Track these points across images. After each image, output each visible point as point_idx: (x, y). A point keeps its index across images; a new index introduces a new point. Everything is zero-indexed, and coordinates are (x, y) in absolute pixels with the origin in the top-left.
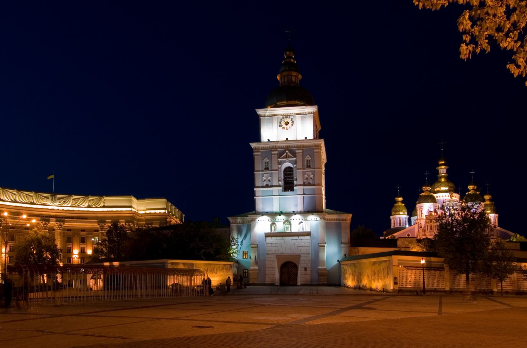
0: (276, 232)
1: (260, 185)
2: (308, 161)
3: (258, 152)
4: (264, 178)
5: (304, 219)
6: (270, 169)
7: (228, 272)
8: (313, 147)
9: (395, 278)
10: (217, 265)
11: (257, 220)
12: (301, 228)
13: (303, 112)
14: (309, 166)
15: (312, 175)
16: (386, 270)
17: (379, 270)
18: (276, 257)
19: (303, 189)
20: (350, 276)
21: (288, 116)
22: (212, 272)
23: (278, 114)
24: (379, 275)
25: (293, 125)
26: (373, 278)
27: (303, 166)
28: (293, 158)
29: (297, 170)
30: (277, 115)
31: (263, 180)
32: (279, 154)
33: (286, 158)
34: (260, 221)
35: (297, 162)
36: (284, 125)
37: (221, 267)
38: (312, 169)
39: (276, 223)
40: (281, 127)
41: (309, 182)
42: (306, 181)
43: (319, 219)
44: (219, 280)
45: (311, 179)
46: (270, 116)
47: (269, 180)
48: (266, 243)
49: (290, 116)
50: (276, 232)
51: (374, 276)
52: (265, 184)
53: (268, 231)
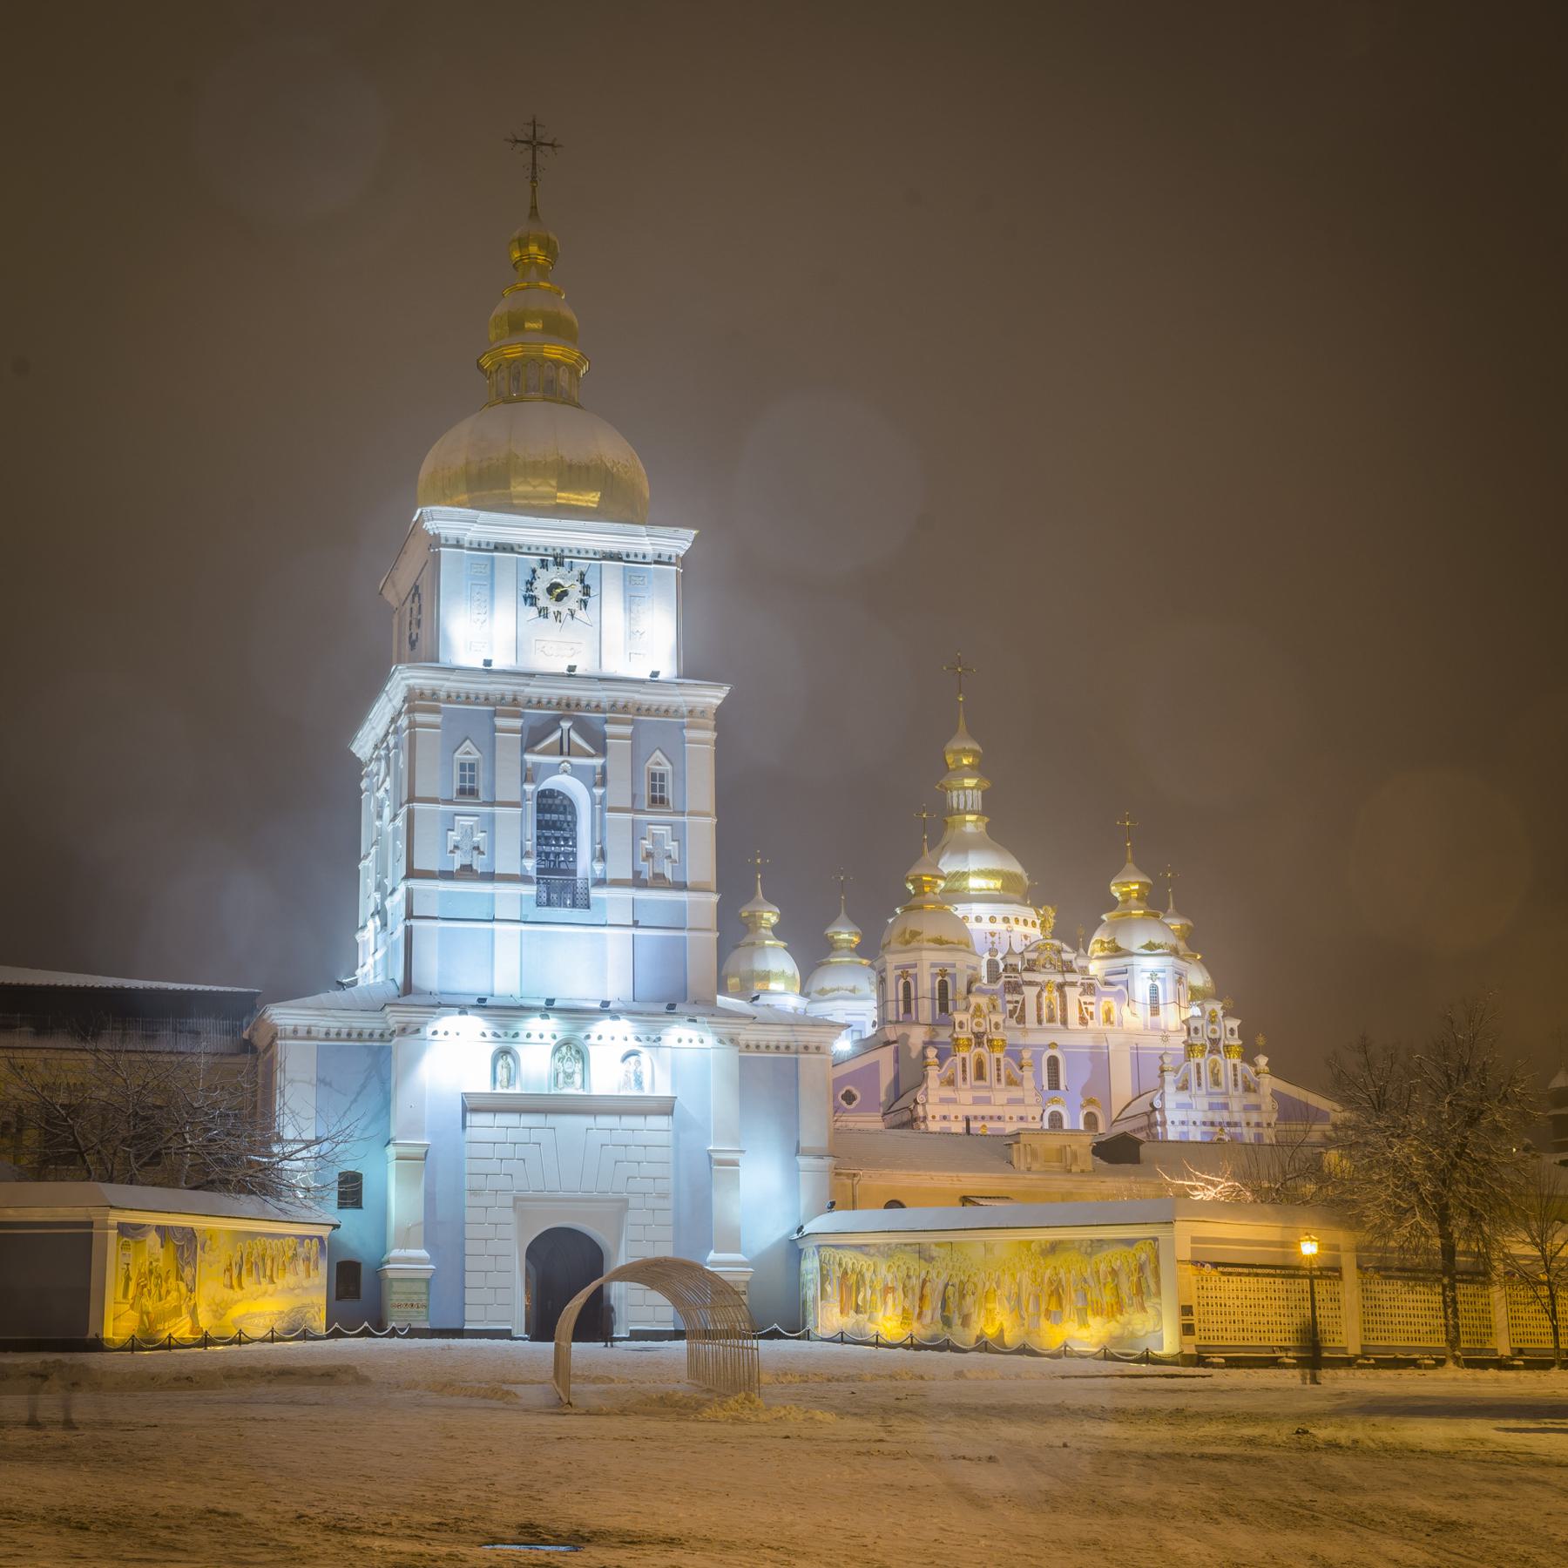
0: (518, 1091)
1: (435, 866)
2: (657, 779)
3: (436, 711)
4: (454, 837)
5: (648, 1039)
6: (483, 796)
7: (311, 1272)
8: (683, 717)
9: (1187, 1310)
10: (276, 1241)
11: (429, 1030)
12: (633, 1078)
13: (632, 549)
14: (658, 801)
15: (675, 843)
16: (1135, 1279)
17: (1085, 1274)
18: (514, 1207)
19: (633, 899)
20: (890, 1297)
21: (566, 560)
22: (258, 1274)
23: (520, 547)
24: (1085, 1295)
25: (586, 606)
26: (1047, 1310)
27: (634, 796)
28: (590, 756)
29: (608, 815)
30: (516, 549)
31: (450, 847)
32: (526, 732)
33: (561, 753)
34: (440, 1036)
35: (609, 776)
37: (290, 1247)
38: (675, 813)
39: (519, 1049)
40: (531, 605)
41: (657, 870)
42: (647, 870)
43: (710, 1040)
44: (282, 1312)
45: (670, 857)
46: (483, 546)
47: (477, 848)
48: (467, 1138)
49: (573, 560)
50: (517, 1089)
51: (1054, 1299)
52: (457, 866)
53: (480, 1083)
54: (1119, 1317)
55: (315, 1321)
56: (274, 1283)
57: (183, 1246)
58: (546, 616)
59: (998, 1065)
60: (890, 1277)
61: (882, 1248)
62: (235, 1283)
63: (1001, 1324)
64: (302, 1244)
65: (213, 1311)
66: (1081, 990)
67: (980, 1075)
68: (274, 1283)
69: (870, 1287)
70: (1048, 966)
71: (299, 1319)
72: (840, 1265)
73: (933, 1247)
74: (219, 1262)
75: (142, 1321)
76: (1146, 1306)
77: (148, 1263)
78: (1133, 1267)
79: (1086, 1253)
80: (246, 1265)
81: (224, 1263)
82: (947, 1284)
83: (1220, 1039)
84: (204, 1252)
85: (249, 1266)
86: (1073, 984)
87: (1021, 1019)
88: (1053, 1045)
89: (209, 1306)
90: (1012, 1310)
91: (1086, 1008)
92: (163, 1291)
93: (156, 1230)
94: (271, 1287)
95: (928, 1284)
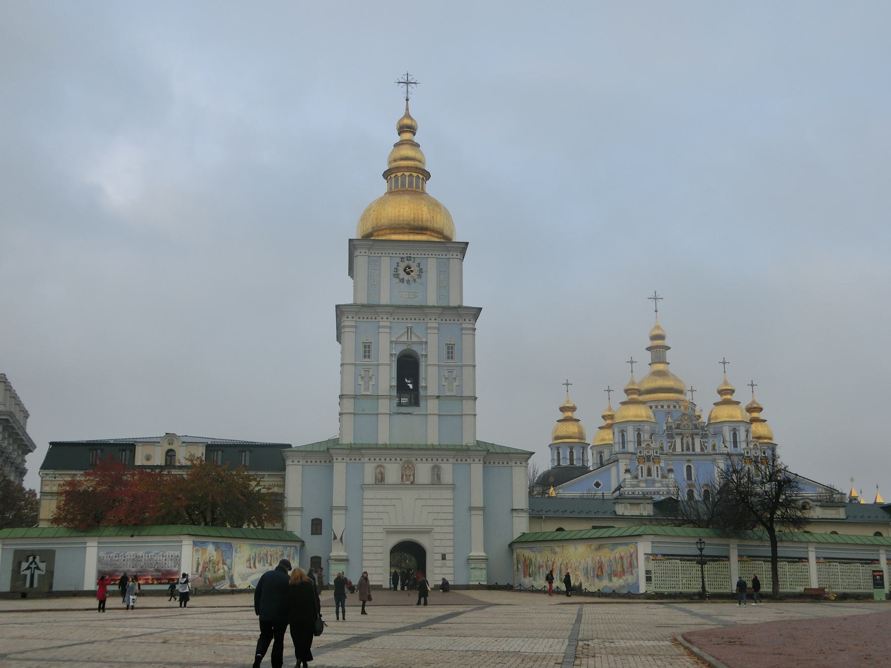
16: (629, 560)
17: (611, 559)
26: (597, 574)
36: (403, 275)
51: (600, 569)
54: (623, 577)
56: (272, 565)
57: (226, 550)
58: (403, 282)
59: (657, 470)
60: (541, 561)
61: (538, 549)
62: (252, 566)
63: (581, 581)
64: (286, 550)
65: (241, 577)
66: (700, 436)
67: (649, 474)
68: (272, 565)
69: (534, 565)
70: (686, 426)
72: (523, 556)
73: (556, 548)
74: (244, 557)
76: (633, 572)
77: (208, 558)
78: (628, 555)
79: (611, 549)
81: (246, 557)
82: (561, 564)
83: (758, 456)
84: (236, 553)
86: (697, 434)
87: (674, 449)
88: (689, 461)
89: (239, 575)
90: (585, 575)
91: (704, 444)
92: (216, 569)
95: (555, 564)
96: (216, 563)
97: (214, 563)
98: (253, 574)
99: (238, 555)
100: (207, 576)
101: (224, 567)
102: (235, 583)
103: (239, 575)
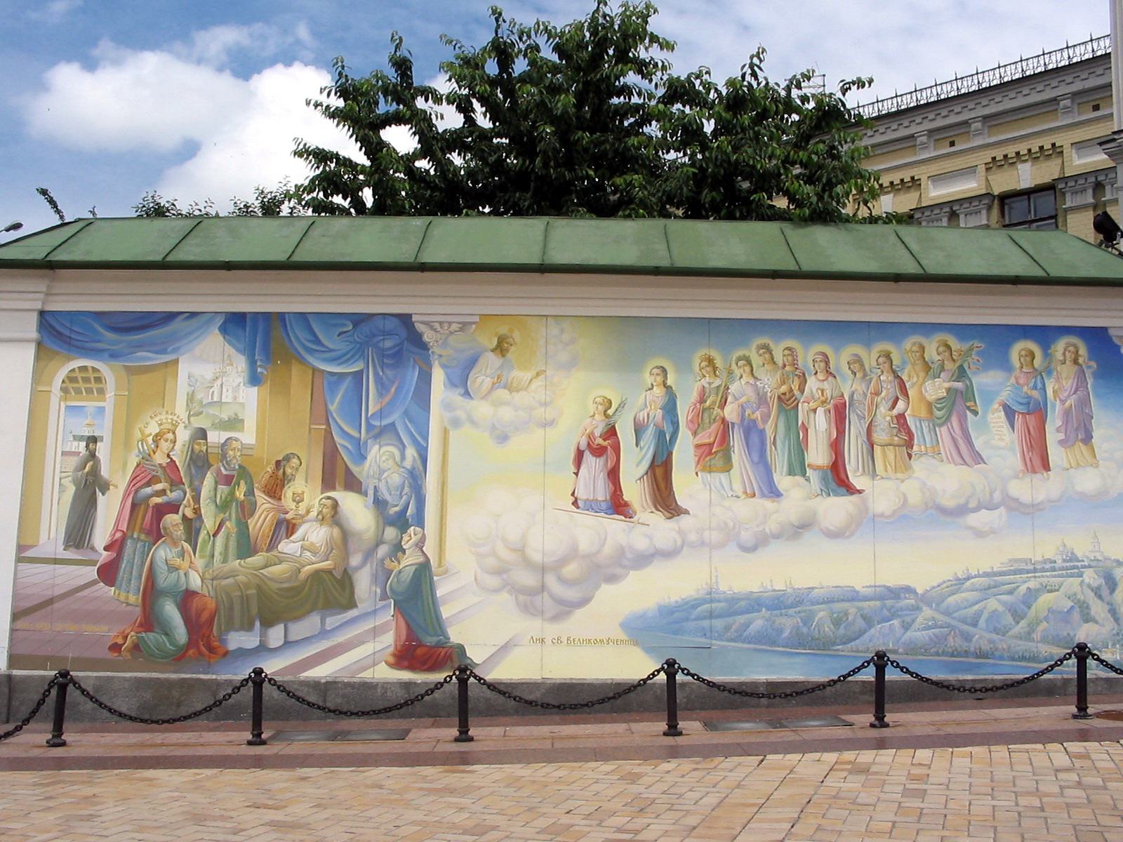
7: (1056, 454)
10: (853, 349)
55: (1087, 618)
56: (850, 490)
57: (358, 376)
62: (634, 488)
65: (517, 590)
68: (850, 490)
71: (994, 615)
74: (547, 424)
75: (150, 620)
77: (183, 436)
80: (696, 427)
84: (467, 394)
85: (706, 437)
89: (499, 571)
92: (260, 521)
93: (224, 330)
94: (836, 508)
96: (262, 475)
97: (244, 472)
98: (643, 560)
99: (482, 409)
100: (164, 579)
101: (335, 505)
102: (455, 635)
103: (499, 571)
